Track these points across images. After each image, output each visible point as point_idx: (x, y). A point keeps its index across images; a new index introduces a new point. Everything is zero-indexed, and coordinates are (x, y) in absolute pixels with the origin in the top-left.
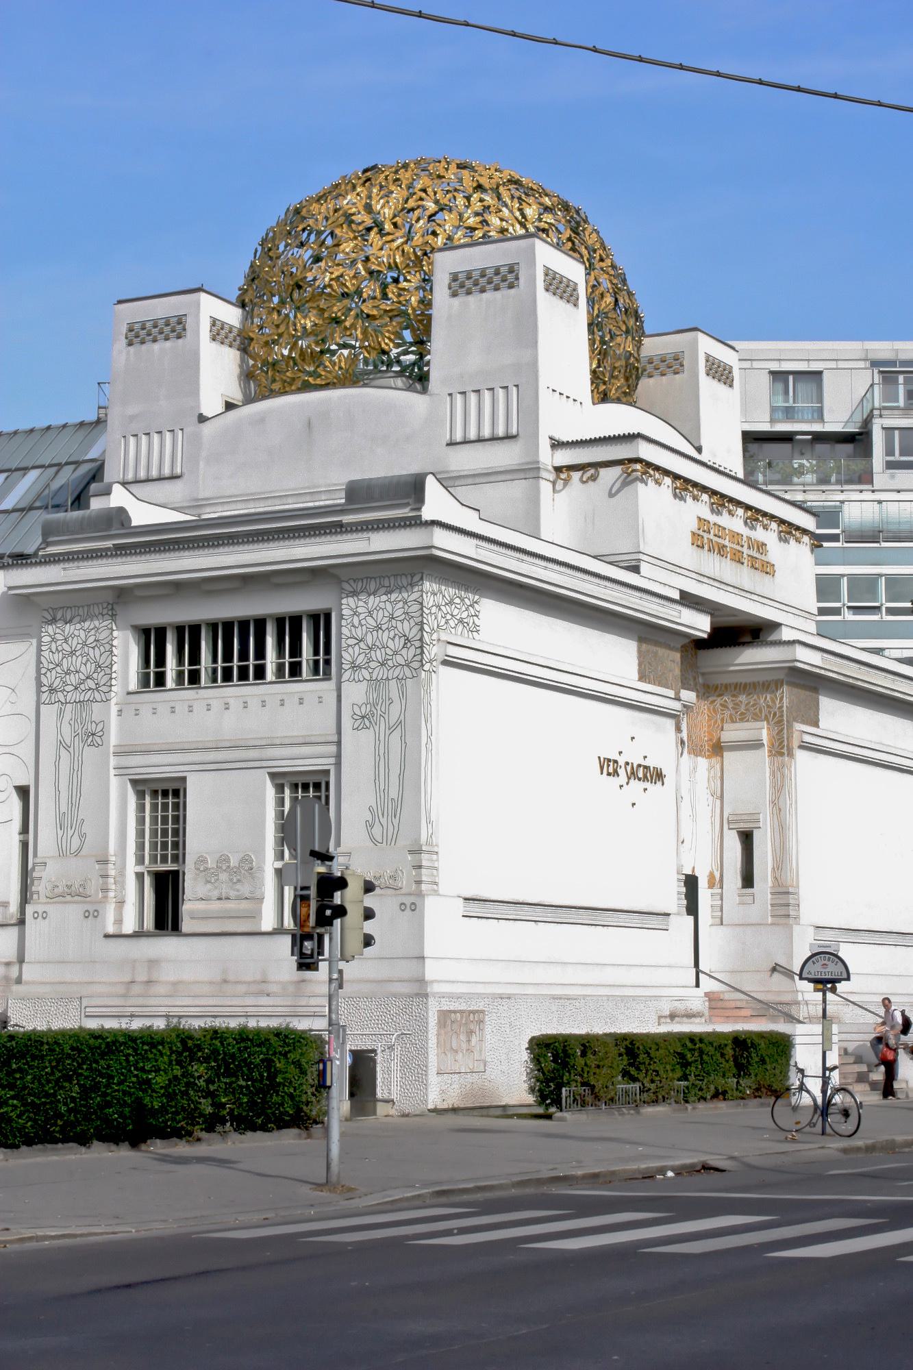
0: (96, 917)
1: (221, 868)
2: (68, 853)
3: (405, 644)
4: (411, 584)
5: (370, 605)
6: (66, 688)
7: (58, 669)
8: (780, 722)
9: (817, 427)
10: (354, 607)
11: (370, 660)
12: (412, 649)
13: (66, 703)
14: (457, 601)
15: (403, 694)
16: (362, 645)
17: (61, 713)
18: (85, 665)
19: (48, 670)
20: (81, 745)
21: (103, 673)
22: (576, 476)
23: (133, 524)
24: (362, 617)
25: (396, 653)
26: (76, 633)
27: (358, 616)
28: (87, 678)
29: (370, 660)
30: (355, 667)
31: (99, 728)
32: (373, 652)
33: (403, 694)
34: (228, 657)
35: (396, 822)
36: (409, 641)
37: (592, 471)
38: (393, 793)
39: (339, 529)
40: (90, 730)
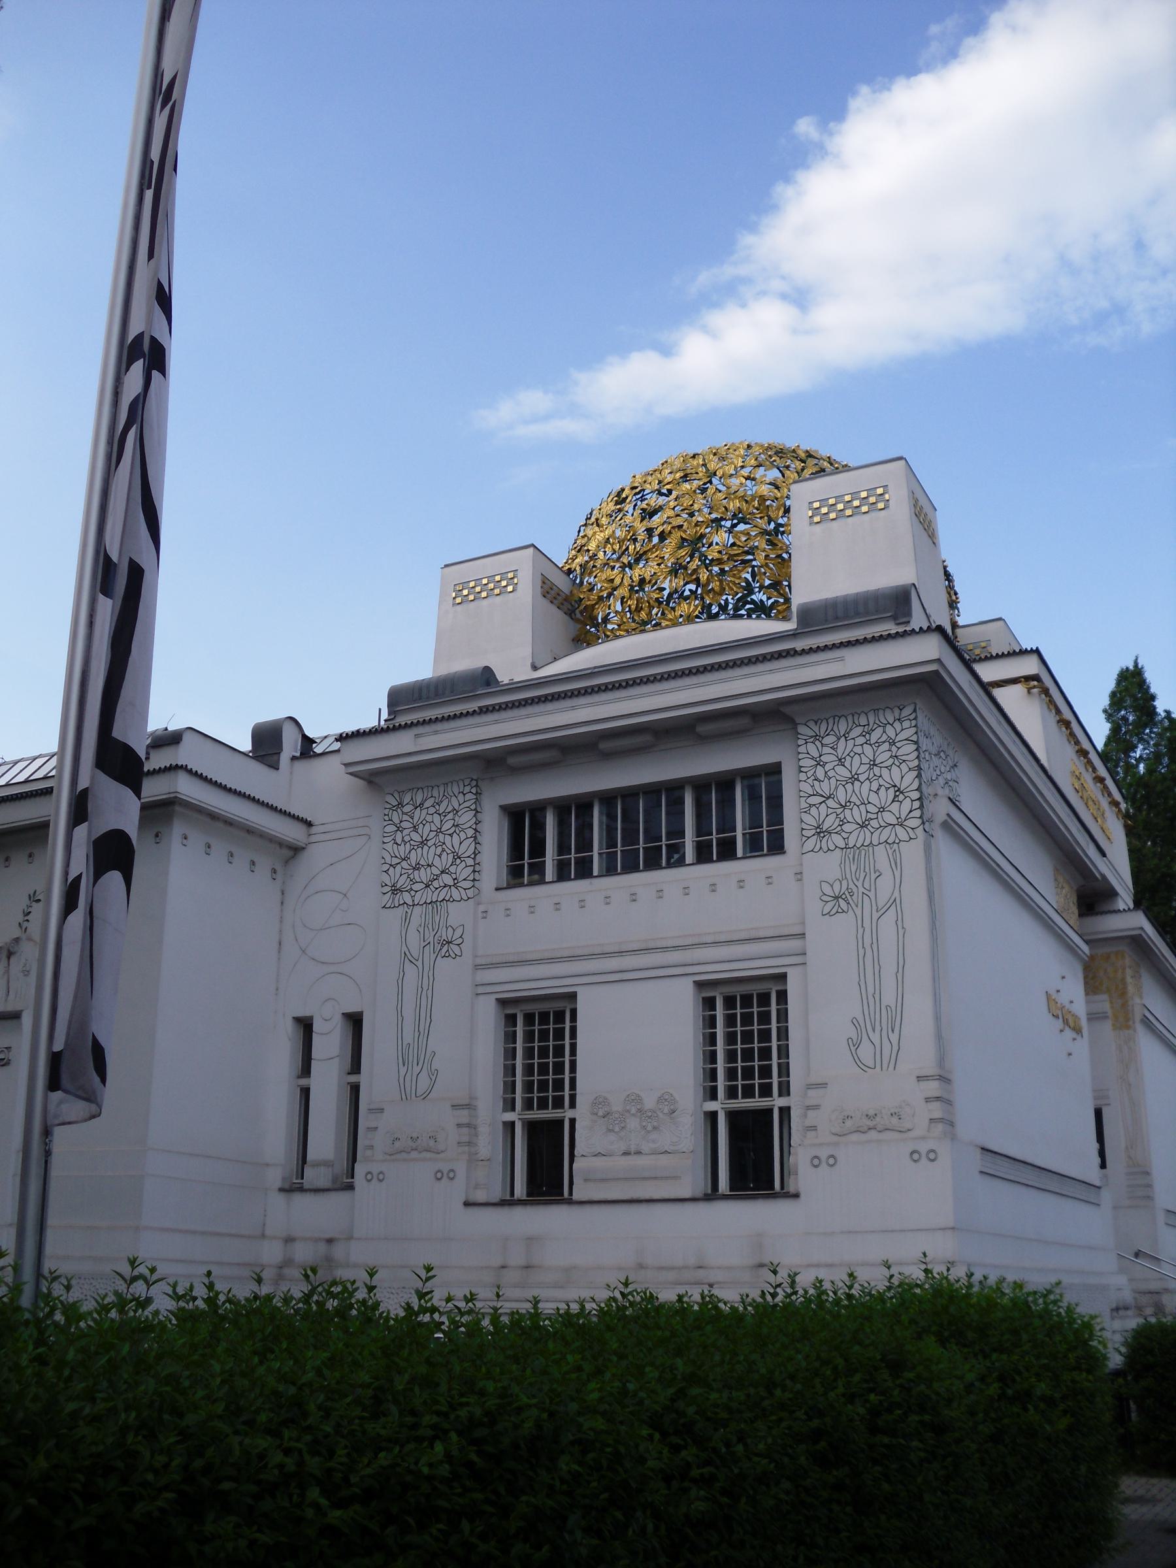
0: (452, 1179)
1: (628, 1111)
2: (413, 1095)
3: (896, 796)
4: (899, 720)
5: (840, 751)
6: (416, 887)
7: (404, 864)
10: (816, 755)
11: (843, 822)
15: (896, 863)
16: (830, 802)
17: (407, 919)
18: (440, 856)
19: (391, 865)
20: (433, 957)
24: (827, 767)
26: (429, 818)
28: (442, 872)
31: (458, 933)
32: (847, 812)
34: (630, 836)
35: (894, 1038)
36: (902, 793)
38: (889, 998)
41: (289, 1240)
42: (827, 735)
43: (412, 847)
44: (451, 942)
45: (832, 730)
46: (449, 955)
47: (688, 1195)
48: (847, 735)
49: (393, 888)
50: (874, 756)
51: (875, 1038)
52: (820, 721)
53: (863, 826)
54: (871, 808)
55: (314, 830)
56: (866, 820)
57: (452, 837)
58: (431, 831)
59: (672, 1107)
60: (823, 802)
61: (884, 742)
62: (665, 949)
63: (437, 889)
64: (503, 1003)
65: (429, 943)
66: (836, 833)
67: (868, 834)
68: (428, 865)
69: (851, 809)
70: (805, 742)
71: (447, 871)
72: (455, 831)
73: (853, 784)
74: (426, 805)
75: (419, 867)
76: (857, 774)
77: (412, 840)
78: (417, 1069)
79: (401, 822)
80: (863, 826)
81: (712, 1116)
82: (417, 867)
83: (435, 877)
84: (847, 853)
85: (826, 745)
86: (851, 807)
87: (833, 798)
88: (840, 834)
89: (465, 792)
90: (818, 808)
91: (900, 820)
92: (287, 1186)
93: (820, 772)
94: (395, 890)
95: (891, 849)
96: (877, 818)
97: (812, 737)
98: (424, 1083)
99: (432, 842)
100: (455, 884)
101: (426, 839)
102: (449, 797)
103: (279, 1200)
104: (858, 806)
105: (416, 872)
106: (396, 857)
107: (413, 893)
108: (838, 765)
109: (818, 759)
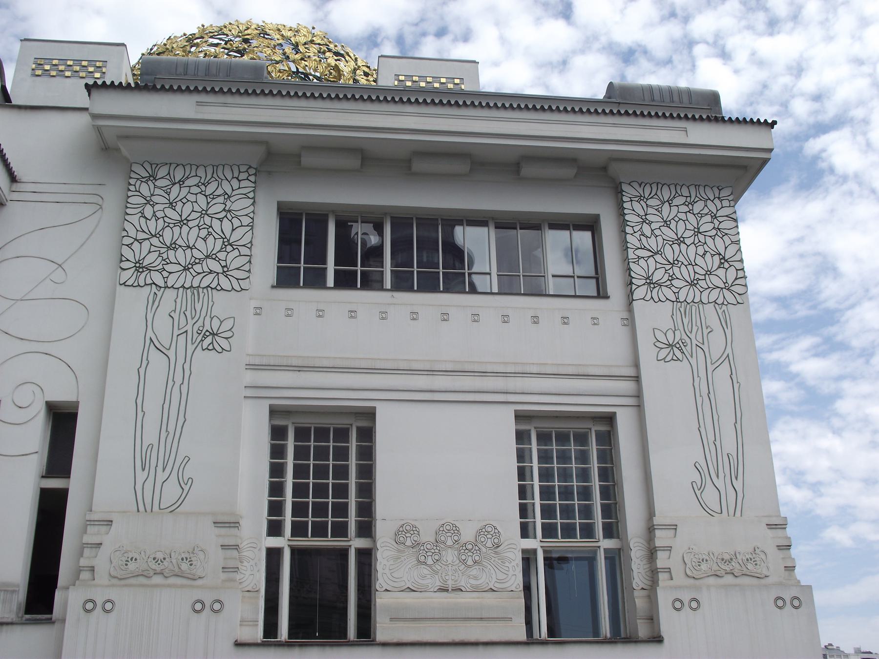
1: (444, 543)
2: (156, 508)
4: (719, 198)
6: (169, 268)
7: (155, 241)
10: (642, 213)
11: (672, 278)
12: (732, 269)
13: (166, 287)
15: (725, 323)
16: (658, 258)
17: (154, 302)
18: (205, 239)
19: (136, 239)
20: (190, 348)
21: (236, 253)
24: (654, 226)
25: (709, 273)
26: (190, 197)
27: (650, 223)
28: (207, 257)
29: (672, 278)
32: (676, 270)
33: (725, 323)
35: (738, 485)
36: (726, 261)
40: (208, 327)
42: (650, 198)
43: (166, 224)
44: (217, 334)
45: (656, 194)
46: (214, 348)
48: (670, 202)
49: (138, 265)
50: (698, 224)
52: (643, 184)
54: (697, 269)
56: (694, 280)
57: (221, 221)
58: (193, 211)
59: (496, 541)
60: (652, 256)
61: (706, 214)
62: (483, 374)
63: (199, 273)
65: (186, 331)
66: (666, 286)
67: (698, 293)
68: (188, 247)
69: (680, 268)
70: (630, 200)
71: (214, 256)
72: (226, 216)
73: (679, 245)
74: (187, 183)
75: (175, 247)
76: (684, 238)
77: (166, 216)
78: (161, 477)
79: (152, 195)
80: (692, 284)
82: (173, 247)
83: (197, 261)
84: (678, 307)
85: (651, 207)
86: (679, 265)
87: (661, 254)
88: (670, 288)
89: (240, 179)
90: (646, 261)
91: (727, 285)
93: (647, 230)
95: (721, 309)
96: (705, 279)
97: (636, 197)
98: (171, 492)
99: (196, 222)
100: (224, 272)
101: (186, 219)
102: (220, 180)
104: (686, 266)
105: (171, 253)
106: (143, 231)
107: (165, 274)
108: (663, 226)
109: (644, 217)
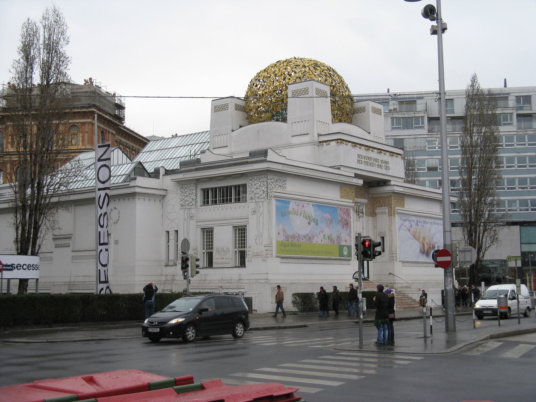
8: (391, 207)
9: (452, 115)
11: (255, 197)
14: (279, 181)
17: (185, 211)
22: (325, 144)
23: (202, 162)
24: (253, 186)
29: (255, 197)
30: (252, 199)
31: (193, 215)
34: (223, 197)
37: (329, 143)
38: (261, 231)
39: (247, 163)
41: (166, 276)
47: (230, 266)
51: (259, 238)
53: (258, 198)
55: (168, 191)
64: (202, 229)
80: (258, 198)
81: (236, 251)
82: (186, 201)
92: (166, 265)
94: (182, 206)
103: (164, 268)
